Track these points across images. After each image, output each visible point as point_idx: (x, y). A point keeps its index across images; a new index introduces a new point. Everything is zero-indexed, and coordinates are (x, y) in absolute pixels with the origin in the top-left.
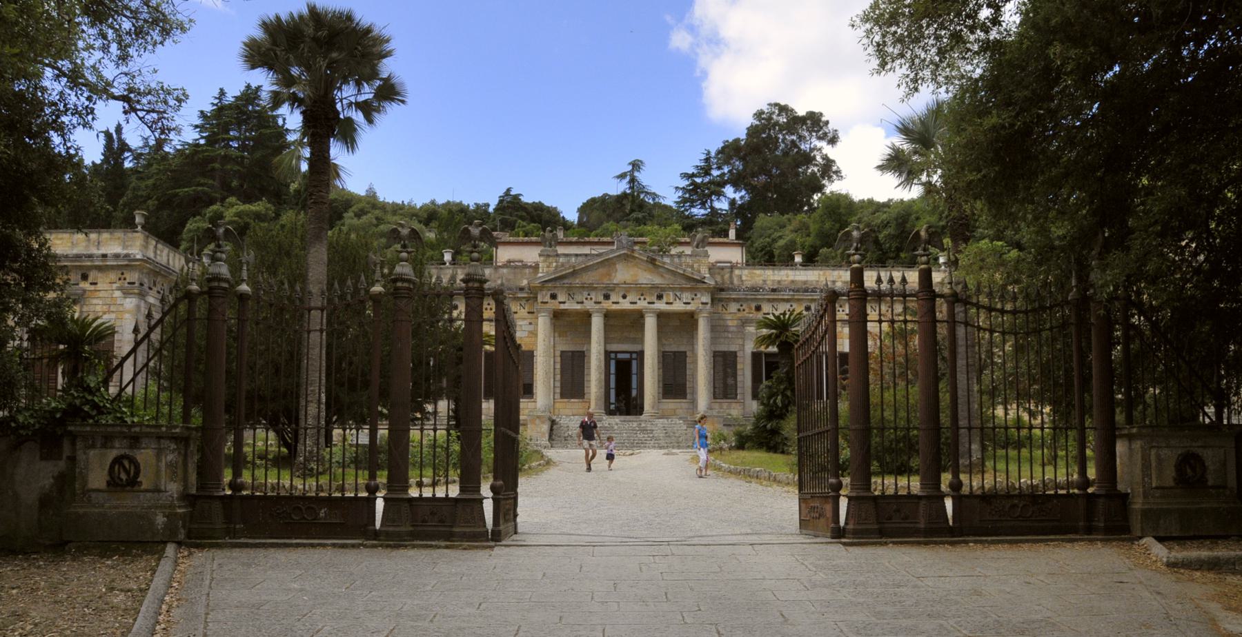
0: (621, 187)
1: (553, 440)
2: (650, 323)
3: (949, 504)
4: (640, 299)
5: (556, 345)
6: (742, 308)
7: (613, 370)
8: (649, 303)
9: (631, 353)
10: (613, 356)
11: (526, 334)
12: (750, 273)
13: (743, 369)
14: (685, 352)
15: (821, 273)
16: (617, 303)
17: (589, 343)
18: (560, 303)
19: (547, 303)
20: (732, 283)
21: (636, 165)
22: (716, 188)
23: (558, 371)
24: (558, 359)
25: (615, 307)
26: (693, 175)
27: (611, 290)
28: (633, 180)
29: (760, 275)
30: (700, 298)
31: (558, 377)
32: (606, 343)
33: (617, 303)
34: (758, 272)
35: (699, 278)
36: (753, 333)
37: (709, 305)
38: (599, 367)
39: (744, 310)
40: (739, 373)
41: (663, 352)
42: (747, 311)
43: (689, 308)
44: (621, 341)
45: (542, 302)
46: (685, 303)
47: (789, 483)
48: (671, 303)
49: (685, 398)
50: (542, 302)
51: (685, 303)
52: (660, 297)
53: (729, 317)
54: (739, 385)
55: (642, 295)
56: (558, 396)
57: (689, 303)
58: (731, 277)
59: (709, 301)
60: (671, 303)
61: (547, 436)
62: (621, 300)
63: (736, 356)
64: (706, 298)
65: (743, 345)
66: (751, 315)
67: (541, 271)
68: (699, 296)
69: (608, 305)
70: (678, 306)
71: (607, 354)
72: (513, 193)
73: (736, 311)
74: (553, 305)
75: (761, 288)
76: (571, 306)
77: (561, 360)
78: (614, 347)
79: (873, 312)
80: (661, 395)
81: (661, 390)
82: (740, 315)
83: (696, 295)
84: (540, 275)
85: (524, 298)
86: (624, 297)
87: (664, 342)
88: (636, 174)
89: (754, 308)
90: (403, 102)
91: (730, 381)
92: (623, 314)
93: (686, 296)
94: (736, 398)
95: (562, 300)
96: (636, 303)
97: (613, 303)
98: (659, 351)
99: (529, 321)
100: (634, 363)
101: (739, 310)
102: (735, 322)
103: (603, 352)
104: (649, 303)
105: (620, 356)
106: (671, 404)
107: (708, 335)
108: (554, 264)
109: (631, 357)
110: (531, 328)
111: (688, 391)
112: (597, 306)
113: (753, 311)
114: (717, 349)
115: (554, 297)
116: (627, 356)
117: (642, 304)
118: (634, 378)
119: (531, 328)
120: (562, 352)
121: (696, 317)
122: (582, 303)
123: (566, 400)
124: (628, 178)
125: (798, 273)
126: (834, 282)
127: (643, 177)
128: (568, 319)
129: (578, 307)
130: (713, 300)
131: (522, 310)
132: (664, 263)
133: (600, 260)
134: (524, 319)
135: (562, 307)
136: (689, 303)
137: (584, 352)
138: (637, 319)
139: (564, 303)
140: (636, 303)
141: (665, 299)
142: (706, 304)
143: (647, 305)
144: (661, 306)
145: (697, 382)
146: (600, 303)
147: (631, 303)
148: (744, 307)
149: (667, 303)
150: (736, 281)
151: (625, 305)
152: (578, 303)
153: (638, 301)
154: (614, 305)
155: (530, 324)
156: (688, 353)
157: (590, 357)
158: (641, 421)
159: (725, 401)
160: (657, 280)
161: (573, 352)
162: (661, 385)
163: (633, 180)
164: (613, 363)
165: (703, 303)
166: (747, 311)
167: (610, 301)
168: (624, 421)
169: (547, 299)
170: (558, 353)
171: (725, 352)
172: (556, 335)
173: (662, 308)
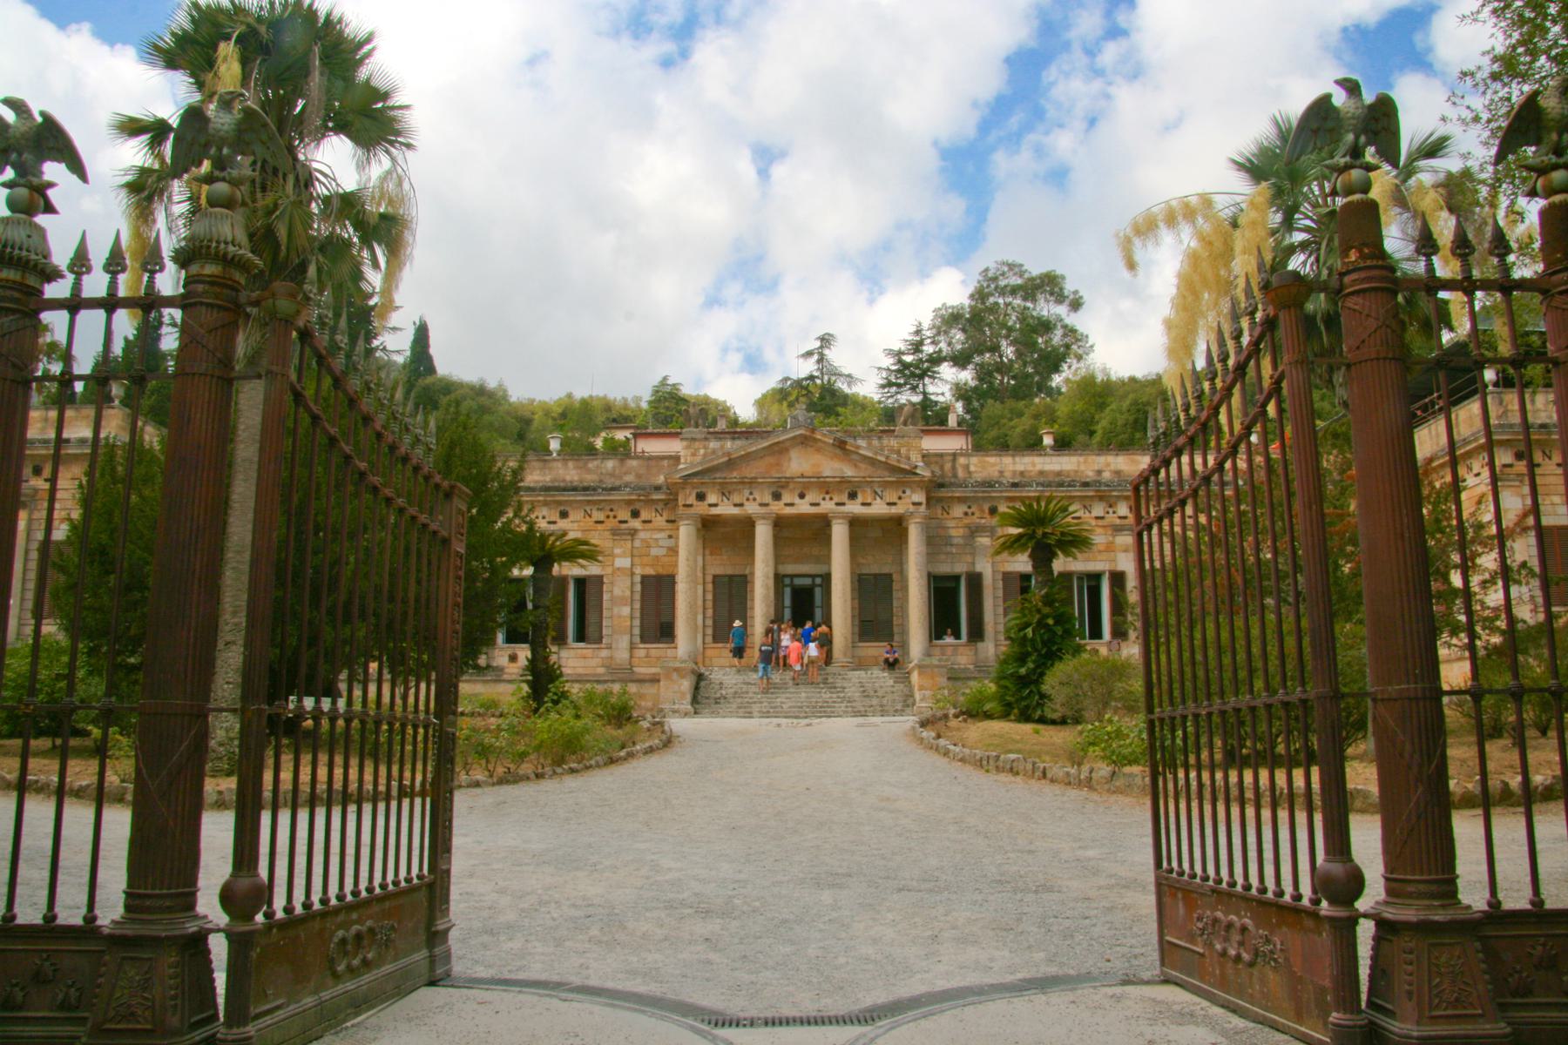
0: (807, 368)
1: (698, 703)
2: (839, 533)
5: (708, 567)
6: (970, 511)
7: (787, 602)
8: (837, 504)
9: (813, 576)
10: (787, 581)
11: (663, 552)
14: (891, 575)
15: (1081, 459)
16: (792, 505)
17: (752, 563)
18: (710, 505)
19: (691, 506)
20: (955, 476)
23: (710, 604)
24: (710, 587)
25: (788, 511)
26: (900, 353)
27: (783, 487)
29: (993, 465)
31: (710, 612)
33: (792, 505)
34: (992, 460)
35: (907, 467)
36: (987, 547)
38: (766, 597)
41: (860, 575)
42: (977, 514)
43: (894, 510)
44: (798, 560)
45: (685, 506)
46: (889, 504)
47: (1070, 783)
48: (869, 504)
50: (685, 506)
51: (889, 504)
52: (853, 496)
55: (827, 493)
56: (709, 639)
57: (894, 504)
58: (954, 468)
59: (924, 501)
61: (689, 698)
62: (797, 500)
64: (919, 497)
67: (682, 460)
68: (908, 492)
69: (778, 508)
70: (879, 508)
71: (779, 579)
72: (670, 382)
74: (701, 509)
76: (726, 509)
78: (790, 569)
80: (857, 637)
81: (857, 629)
84: (681, 466)
86: (802, 496)
87: (862, 561)
88: (826, 352)
90: (409, 146)
92: (801, 521)
93: (891, 496)
96: (818, 504)
97: (786, 505)
98: (852, 573)
99: (668, 533)
100: (818, 591)
101: (966, 514)
102: (961, 530)
103: (771, 575)
104: (837, 504)
105: (798, 581)
107: (923, 549)
108: (702, 451)
110: (671, 543)
111: (896, 630)
112: (763, 510)
113: (987, 515)
116: (808, 581)
117: (827, 506)
119: (671, 543)
120: (715, 577)
121: (904, 524)
122: (741, 505)
123: (720, 645)
124: (816, 357)
125: (1047, 459)
126: (1099, 472)
129: (736, 511)
130: (928, 499)
131: (659, 518)
132: (858, 447)
133: (766, 444)
135: (714, 511)
136: (894, 504)
137: (745, 576)
138: (818, 528)
139: (715, 505)
140: (818, 504)
141: (860, 499)
142: (919, 504)
143: (834, 507)
144: (855, 508)
145: (908, 616)
146: (767, 505)
147: (812, 505)
149: (863, 504)
150: (961, 473)
151: (803, 507)
152: (735, 505)
153: (822, 502)
155: (670, 537)
156: (894, 577)
157: (753, 583)
160: (849, 472)
161: (731, 577)
162: (857, 623)
163: (821, 360)
164: (788, 591)
165: (914, 504)
166: (977, 514)
169: (692, 500)
170: (709, 578)
172: (707, 552)
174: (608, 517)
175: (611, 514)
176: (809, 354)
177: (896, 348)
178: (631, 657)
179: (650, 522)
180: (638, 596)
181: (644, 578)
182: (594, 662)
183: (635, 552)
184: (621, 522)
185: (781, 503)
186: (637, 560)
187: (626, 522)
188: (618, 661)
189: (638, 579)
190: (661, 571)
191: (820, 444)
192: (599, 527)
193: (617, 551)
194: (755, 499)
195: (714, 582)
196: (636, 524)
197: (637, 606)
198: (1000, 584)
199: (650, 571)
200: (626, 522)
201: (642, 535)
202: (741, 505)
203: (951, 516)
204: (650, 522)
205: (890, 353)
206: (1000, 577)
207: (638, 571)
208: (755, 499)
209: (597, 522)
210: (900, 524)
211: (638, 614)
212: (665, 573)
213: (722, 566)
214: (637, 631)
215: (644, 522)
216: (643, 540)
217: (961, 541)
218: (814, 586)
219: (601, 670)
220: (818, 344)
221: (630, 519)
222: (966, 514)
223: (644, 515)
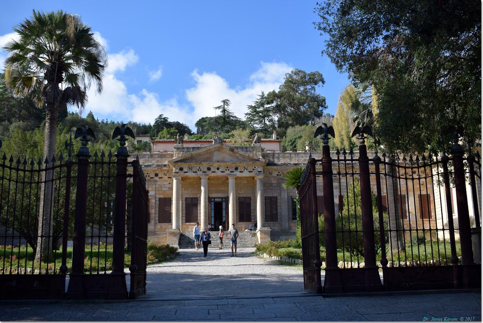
1: (181, 245)
2: (231, 182)
3: (381, 274)
4: (226, 170)
6: (279, 174)
8: (231, 172)
9: (222, 198)
11: (167, 189)
12: (283, 156)
14: (250, 197)
16: (215, 172)
18: (185, 172)
22: (266, 113)
23: (184, 208)
24: (184, 202)
25: (213, 175)
27: (211, 166)
28: (224, 111)
30: (257, 169)
31: (184, 211)
32: (208, 194)
33: (215, 172)
35: (256, 158)
39: (280, 175)
40: (279, 208)
41: (239, 197)
42: (282, 175)
44: (218, 192)
48: (242, 172)
49: (251, 222)
54: (278, 214)
55: (227, 168)
59: (262, 171)
62: (216, 170)
63: (277, 199)
67: (174, 156)
70: (246, 174)
71: (209, 200)
73: (276, 175)
75: (288, 163)
76: (191, 174)
77: (186, 202)
78: (213, 195)
81: (238, 217)
83: (255, 167)
85: (166, 170)
87: (239, 192)
88: (226, 106)
91: (274, 212)
92: (218, 178)
94: (277, 221)
95: (186, 171)
96: (224, 172)
97: (212, 172)
98: (236, 197)
99: (169, 182)
104: (231, 172)
105: (216, 200)
106: (243, 225)
109: (222, 200)
111: (252, 217)
114: (267, 196)
115: (181, 169)
118: (224, 211)
120: (186, 198)
124: (221, 110)
128: (189, 181)
129: (194, 175)
134: (167, 181)
136: (252, 172)
139: (187, 172)
140: (224, 172)
141: (239, 170)
142: (261, 172)
143: (230, 173)
144: (238, 174)
146: (206, 172)
147: (222, 172)
148: (280, 173)
149: (240, 172)
152: (194, 172)
153: (225, 171)
154: (213, 173)
155: (169, 183)
158: (228, 234)
159: (271, 222)
161: (192, 198)
162: (238, 215)
163: (224, 111)
164: (213, 203)
165: (258, 172)
166: (282, 175)
170: (184, 199)
171: (271, 197)
172: (183, 189)
176: (219, 107)
177: (253, 105)
178: (155, 228)
179: (162, 178)
180: (157, 206)
181: (160, 199)
184: (151, 178)
185: (211, 172)
186: (157, 192)
187: (153, 178)
189: (158, 199)
190: (166, 196)
191: (225, 150)
194: (201, 170)
195: (185, 200)
197: (157, 209)
199: (162, 196)
200: (153, 178)
201: (159, 183)
202: (196, 172)
204: (162, 178)
205: (251, 107)
207: (158, 196)
210: (254, 179)
211: (157, 212)
212: (167, 197)
213: (189, 194)
214: (157, 219)
215: (160, 178)
216: (159, 185)
217: (276, 185)
218: (222, 201)
220: (222, 104)
221: (154, 177)
222: (278, 175)
223: (160, 176)
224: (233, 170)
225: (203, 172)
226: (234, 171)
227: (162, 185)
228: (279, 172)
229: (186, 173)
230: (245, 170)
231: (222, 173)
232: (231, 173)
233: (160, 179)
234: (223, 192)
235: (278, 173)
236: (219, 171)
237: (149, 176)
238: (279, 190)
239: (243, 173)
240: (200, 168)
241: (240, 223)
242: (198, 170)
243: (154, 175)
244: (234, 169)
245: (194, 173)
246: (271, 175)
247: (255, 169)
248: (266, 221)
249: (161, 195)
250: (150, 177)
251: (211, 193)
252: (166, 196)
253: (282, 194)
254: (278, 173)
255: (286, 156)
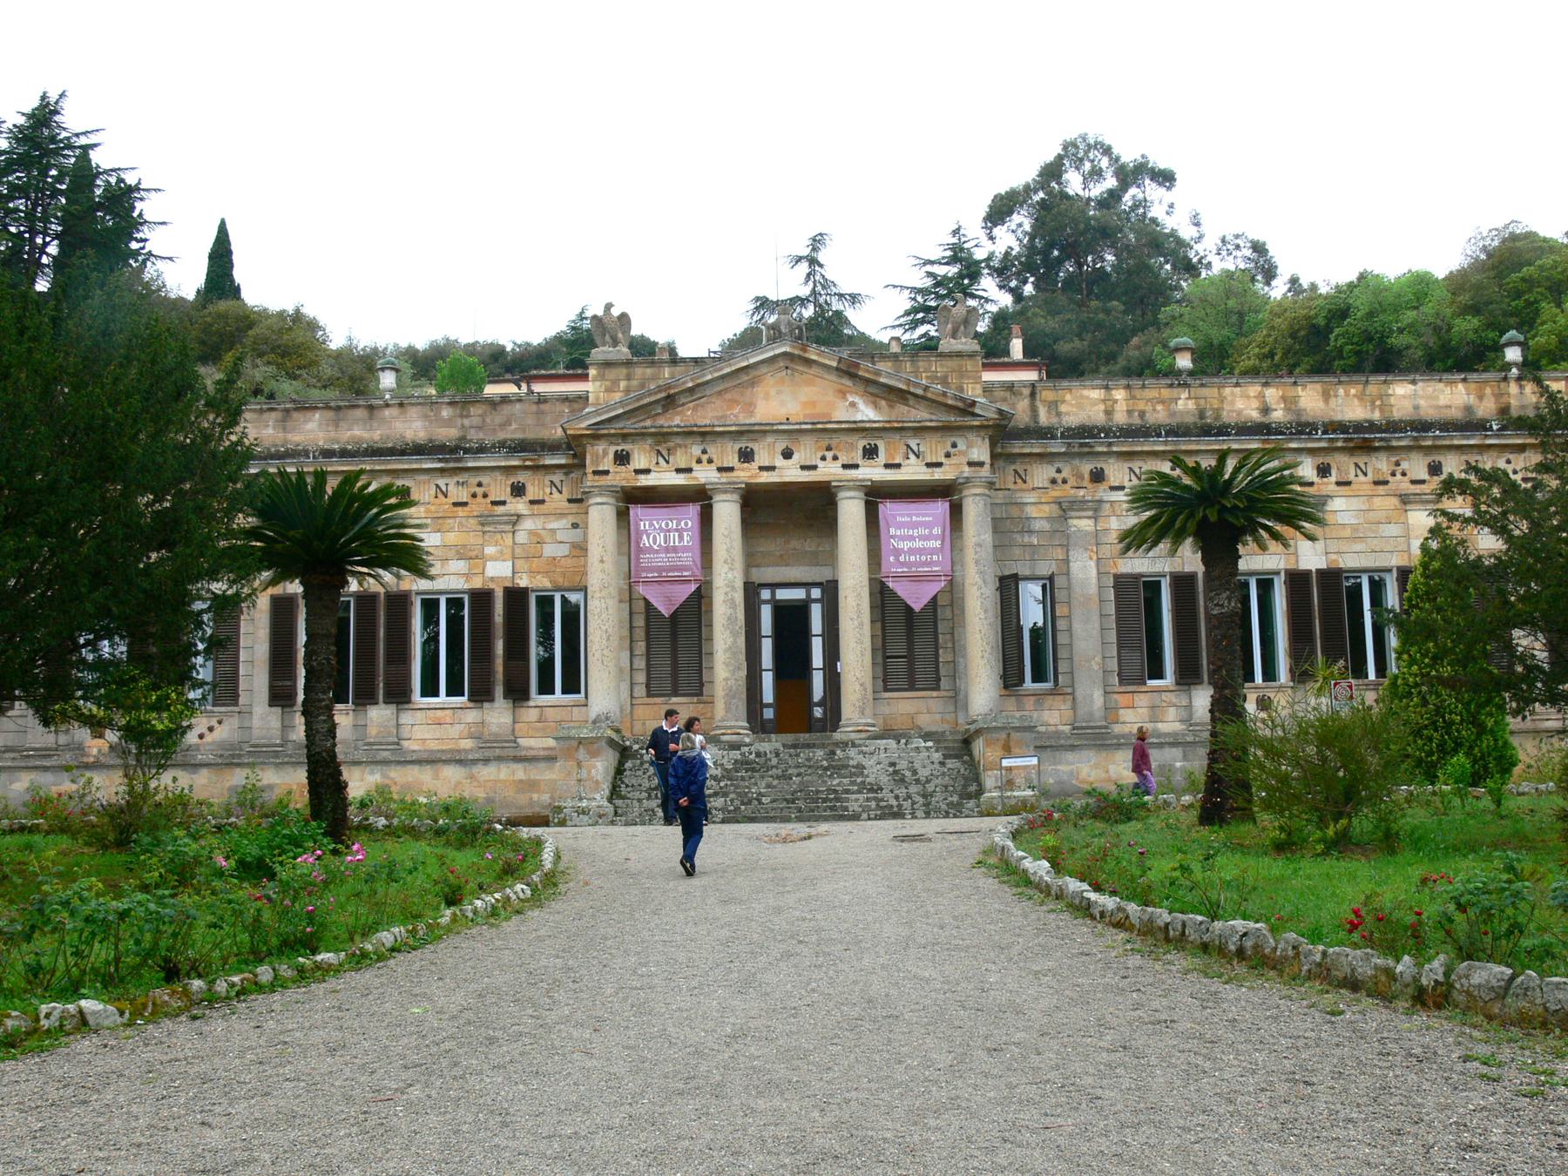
4: (823, 458)
6: (1059, 477)
9: (807, 585)
10: (766, 594)
11: (563, 550)
13: (1069, 617)
16: (772, 468)
18: (638, 472)
19: (607, 472)
21: (817, 242)
23: (640, 634)
25: (766, 478)
33: (772, 468)
36: (1087, 533)
37: (987, 467)
39: (1064, 481)
42: (1072, 482)
45: (595, 473)
48: (898, 466)
50: (595, 473)
51: (929, 465)
52: (871, 452)
53: (1030, 498)
55: (829, 449)
56: (640, 691)
57: (939, 465)
60: (898, 466)
62: (779, 462)
64: (980, 451)
65: (1067, 561)
66: (1082, 492)
68: (962, 446)
69: (747, 474)
73: (1046, 484)
74: (622, 477)
79: (1362, 478)
82: (1056, 493)
83: (954, 445)
86: (787, 454)
89: (1087, 476)
93: (934, 448)
96: (814, 467)
97: (761, 468)
98: (870, 579)
99: (571, 519)
100: (816, 613)
101: (1054, 481)
102: (1046, 508)
103: (739, 584)
104: (845, 466)
105: (783, 594)
107: (988, 537)
108: (623, 384)
109: (808, 594)
110: (575, 535)
112: (725, 478)
113: (1086, 483)
115: (622, 459)
116: (798, 594)
117: (829, 471)
119: (575, 535)
122: (689, 470)
127: (835, 267)
130: (994, 456)
131: (556, 495)
132: (878, 373)
134: (562, 515)
136: (939, 465)
139: (647, 471)
140: (814, 467)
141: (882, 458)
142: (981, 464)
146: (731, 469)
147: (803, 468)
148: (1064, 474)
149: (887, 466)
151: (790, 472)
152: (678, 471)
153: (821, 464)
157: (711, 598)
160: (866, 412)
164: (766, 614)
165: (970, 464)
166: (1072, 482)
167: (755, 465)
168: (795, 746)
169: (607, 463)
173: (877, 478)
174: (474, 496)
175: (480, 491)
179: (542, 502)
182: (454, 731)
183: (518, 551)
184: (494, 503)
187: (503, 503)
188: (494, 729)
192: (460, 511)
193: (490, 550)
196: (519, 506)
198: (1111, 595)
200: (503, 503)
201: (527, 524)
202: (689, 470)
203: (1030, 484)
204: (542, 502)
206: (1111, 582)
208: (710, 461)
209: (455, 504)
215: (532, 502)
217: (1046, 526)
219: (467, 744)
221: (509, 499)
222: (1054, 481)
223: (532, 492)
224: (857, 457)
225: (720, 469)
226: (860, 462)
227: (542, 532)
228: (1059, 471)
229: (642, 477)
230: (912, 456)
231: (806, 473)
232: (848, 472)
233: (536, 507)
234: (814, 559)
235: (1053, 474)
236: (789, 462)
237: (485, 496)
238: (1059, 550)
239: (903, 470)
240: (704, 452)
241: (888, 695)
242: (699, 461)
243: (509, 489)
244: (860, 452)
245: (682, 476)
246: (1025, 482)
247: (953, 451)
248: (1006, 687)
249: (539, 577)
250: (488, 500)
251: (758, 566)
252: (561, 580)
253: (1075, 567)
254: (1053, 474)
255: (1088, 398)
